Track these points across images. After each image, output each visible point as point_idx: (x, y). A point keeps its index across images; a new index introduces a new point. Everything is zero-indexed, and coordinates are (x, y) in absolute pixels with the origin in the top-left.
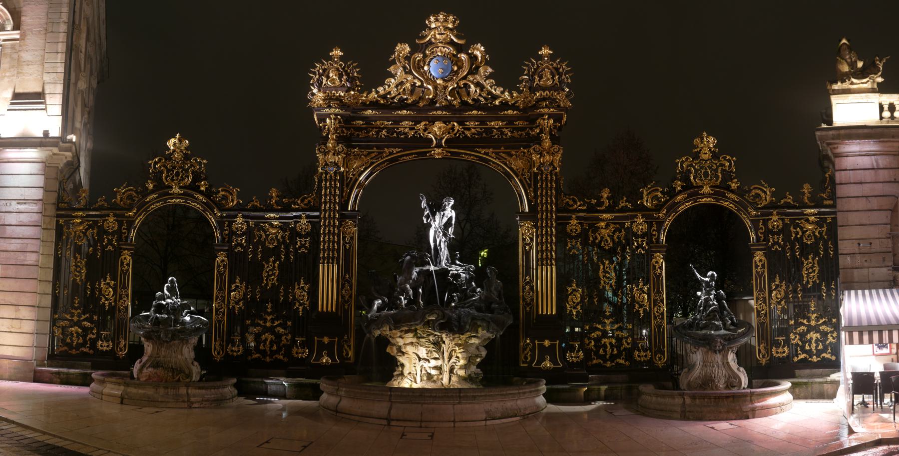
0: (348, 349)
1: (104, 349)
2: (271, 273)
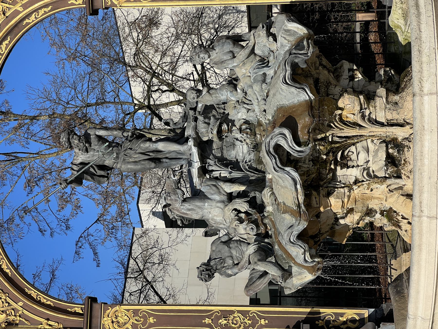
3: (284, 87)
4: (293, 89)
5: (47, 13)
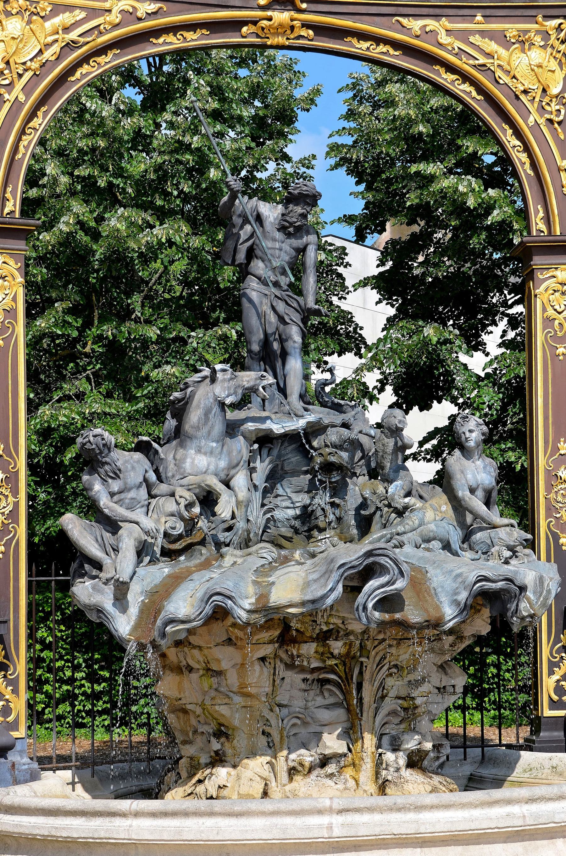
5: (523, 167)
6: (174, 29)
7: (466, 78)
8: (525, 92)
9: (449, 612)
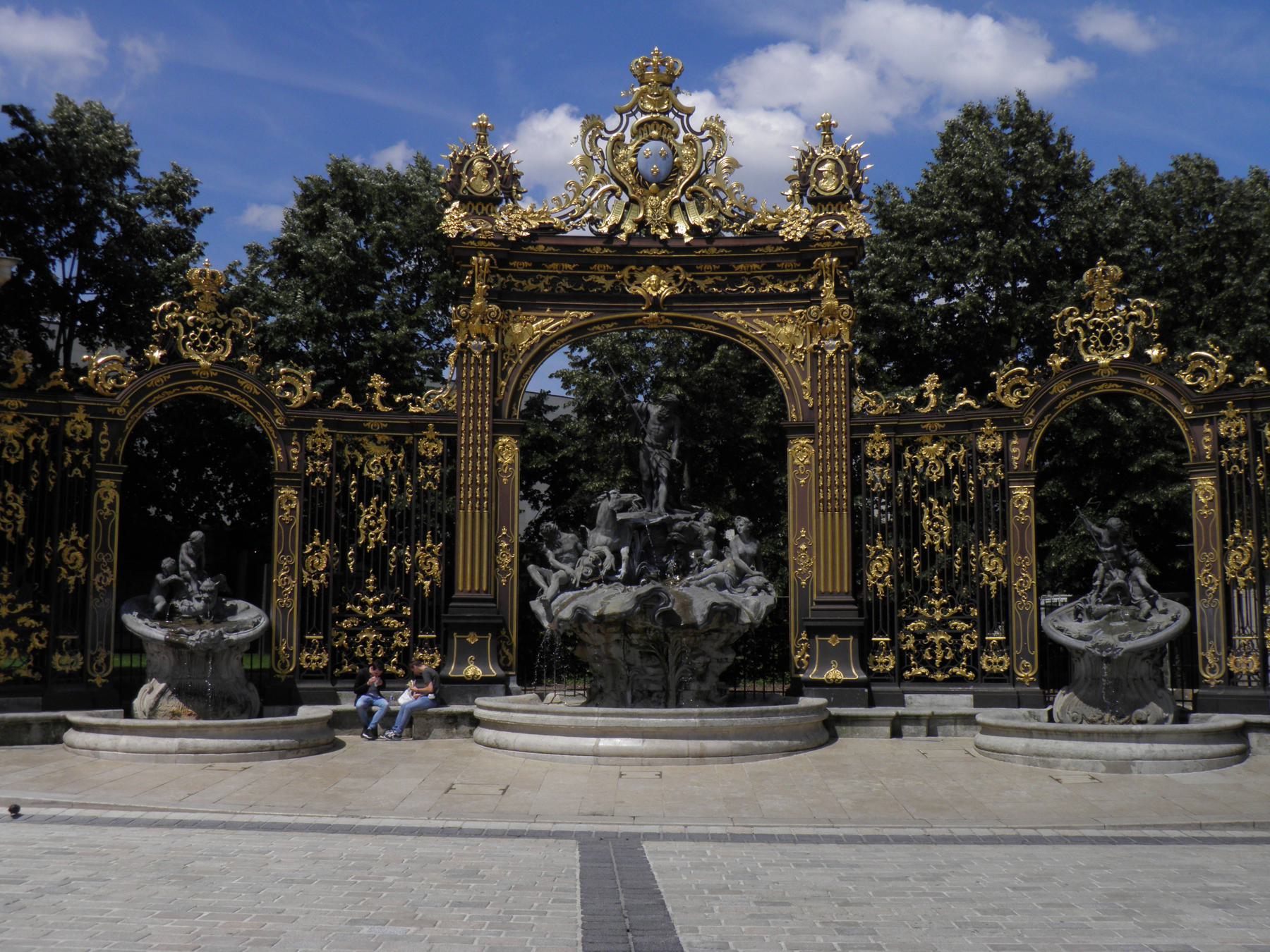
0: (507, 652)
1: (67, 669)
2: (372, 525)
3: (709, 603)
4: (706, 612)
6: (599, 323)
7: (753, 341)
8: (783, 347)
9: (700, 620)
